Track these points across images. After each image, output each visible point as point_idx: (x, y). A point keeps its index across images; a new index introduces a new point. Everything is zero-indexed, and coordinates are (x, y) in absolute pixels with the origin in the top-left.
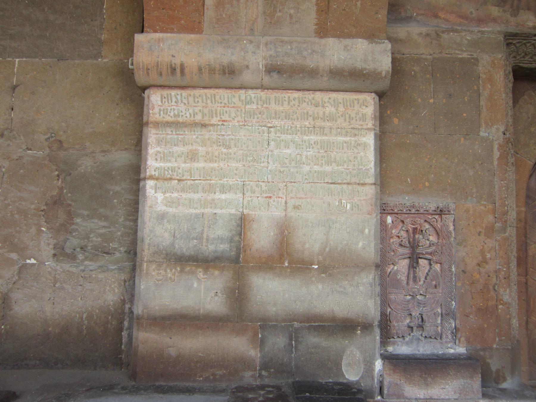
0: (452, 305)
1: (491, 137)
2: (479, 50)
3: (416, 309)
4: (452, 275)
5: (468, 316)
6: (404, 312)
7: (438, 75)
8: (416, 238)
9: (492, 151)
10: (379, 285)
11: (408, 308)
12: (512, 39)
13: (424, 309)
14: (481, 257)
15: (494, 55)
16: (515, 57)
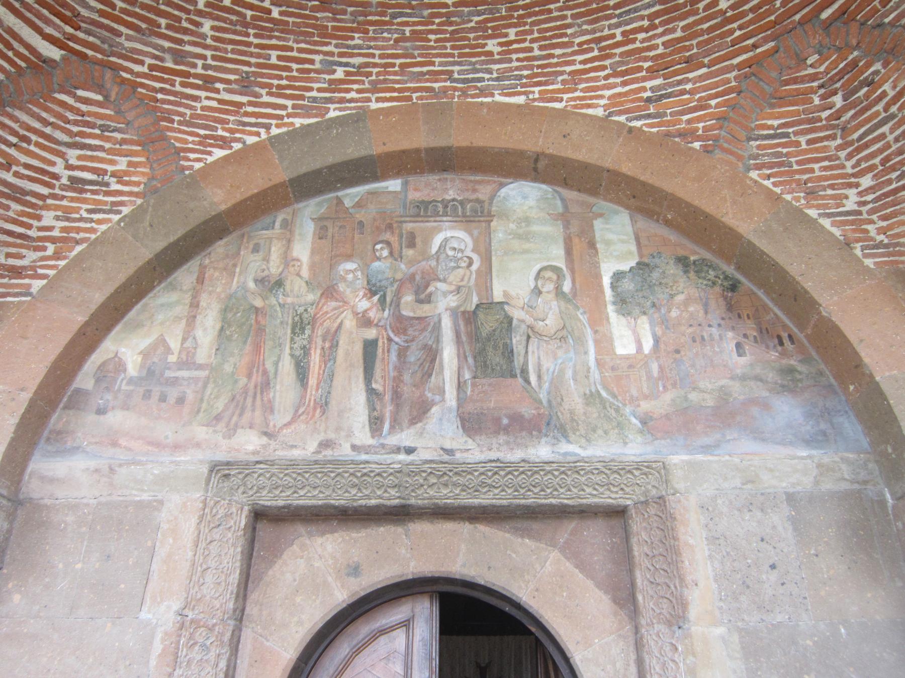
1: (155, 621)
2: (167, 489)
7: (98, 527)
9: (151, 643)
12: (229, 469)
15: (189, 495)
16: (244, 493)
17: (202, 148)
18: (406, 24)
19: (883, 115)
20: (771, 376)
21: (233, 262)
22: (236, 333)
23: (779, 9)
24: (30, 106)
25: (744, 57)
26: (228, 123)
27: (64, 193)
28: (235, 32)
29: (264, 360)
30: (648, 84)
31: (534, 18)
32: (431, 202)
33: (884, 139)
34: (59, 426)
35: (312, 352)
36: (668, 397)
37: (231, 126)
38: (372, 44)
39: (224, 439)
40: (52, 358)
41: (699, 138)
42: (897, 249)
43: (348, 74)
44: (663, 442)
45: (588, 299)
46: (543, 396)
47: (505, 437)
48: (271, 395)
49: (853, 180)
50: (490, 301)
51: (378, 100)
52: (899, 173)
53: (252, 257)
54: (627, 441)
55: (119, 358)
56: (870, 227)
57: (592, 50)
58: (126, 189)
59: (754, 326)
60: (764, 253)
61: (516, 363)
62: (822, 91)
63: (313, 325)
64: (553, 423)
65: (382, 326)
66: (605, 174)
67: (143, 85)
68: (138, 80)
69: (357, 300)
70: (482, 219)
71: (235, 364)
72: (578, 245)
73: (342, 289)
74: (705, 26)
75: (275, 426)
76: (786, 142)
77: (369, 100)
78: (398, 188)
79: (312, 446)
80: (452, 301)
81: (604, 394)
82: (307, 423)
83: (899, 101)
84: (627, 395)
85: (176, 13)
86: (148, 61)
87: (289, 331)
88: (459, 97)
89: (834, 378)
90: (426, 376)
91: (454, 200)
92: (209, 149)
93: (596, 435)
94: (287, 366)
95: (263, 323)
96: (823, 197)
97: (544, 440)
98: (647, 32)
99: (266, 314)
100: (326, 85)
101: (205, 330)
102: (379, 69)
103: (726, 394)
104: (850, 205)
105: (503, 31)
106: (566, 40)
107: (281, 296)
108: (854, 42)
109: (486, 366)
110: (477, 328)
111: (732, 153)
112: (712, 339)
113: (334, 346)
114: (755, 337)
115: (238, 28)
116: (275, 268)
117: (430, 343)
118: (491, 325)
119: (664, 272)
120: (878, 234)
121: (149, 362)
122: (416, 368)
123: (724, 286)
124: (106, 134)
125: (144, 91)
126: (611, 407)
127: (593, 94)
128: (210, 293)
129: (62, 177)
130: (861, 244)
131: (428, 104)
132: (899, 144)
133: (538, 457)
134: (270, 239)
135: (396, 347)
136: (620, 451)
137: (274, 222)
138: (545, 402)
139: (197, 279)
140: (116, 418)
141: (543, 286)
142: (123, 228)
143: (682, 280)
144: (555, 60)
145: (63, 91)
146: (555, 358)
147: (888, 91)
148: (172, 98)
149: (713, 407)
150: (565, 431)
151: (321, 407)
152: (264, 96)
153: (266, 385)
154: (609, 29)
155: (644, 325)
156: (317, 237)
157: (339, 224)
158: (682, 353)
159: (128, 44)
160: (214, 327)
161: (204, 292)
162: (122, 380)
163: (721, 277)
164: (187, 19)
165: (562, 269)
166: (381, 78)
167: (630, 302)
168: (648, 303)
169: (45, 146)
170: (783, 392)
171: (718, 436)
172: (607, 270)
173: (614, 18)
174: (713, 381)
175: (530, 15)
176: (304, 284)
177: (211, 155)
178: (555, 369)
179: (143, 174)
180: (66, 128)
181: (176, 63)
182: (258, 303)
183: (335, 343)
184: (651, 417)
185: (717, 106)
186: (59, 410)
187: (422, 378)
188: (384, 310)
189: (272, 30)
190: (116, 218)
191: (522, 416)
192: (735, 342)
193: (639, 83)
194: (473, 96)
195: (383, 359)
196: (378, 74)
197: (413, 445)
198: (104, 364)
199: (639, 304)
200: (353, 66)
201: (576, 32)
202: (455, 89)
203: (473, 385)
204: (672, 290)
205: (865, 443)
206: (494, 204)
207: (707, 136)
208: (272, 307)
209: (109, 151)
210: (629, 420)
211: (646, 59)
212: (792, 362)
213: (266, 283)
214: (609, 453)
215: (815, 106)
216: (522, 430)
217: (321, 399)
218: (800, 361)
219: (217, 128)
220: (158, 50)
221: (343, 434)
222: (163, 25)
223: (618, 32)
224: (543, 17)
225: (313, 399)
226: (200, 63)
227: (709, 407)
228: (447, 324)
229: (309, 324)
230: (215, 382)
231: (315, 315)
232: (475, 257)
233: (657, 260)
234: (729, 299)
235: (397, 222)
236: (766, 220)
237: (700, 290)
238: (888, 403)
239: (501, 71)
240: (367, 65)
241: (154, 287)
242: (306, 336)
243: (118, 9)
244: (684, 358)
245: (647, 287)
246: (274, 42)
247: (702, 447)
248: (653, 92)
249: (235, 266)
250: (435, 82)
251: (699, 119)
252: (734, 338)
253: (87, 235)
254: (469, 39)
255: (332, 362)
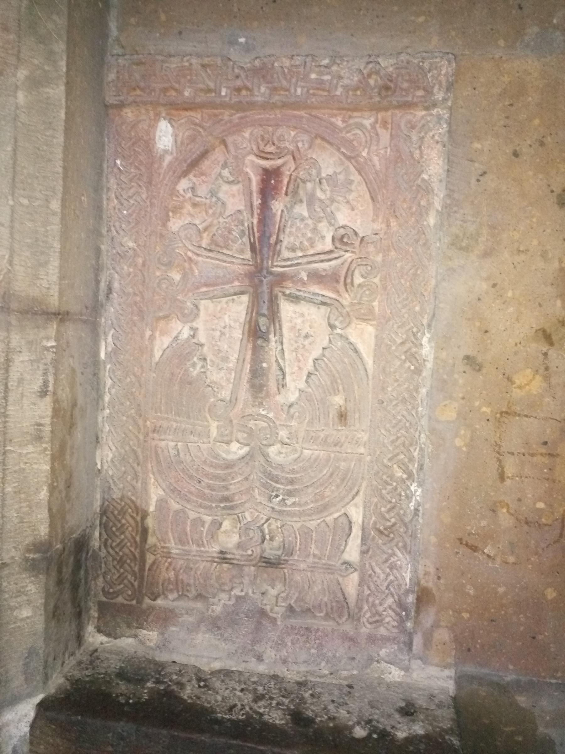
0: (409, 498)
3: (259, 498)
4: (418, 371)
5: (474, 549)
6: (211, 507)
8: (275, 215)
10: (43, 393)
11: (226, 493)
13: (289, 502)
14: (559, 303)
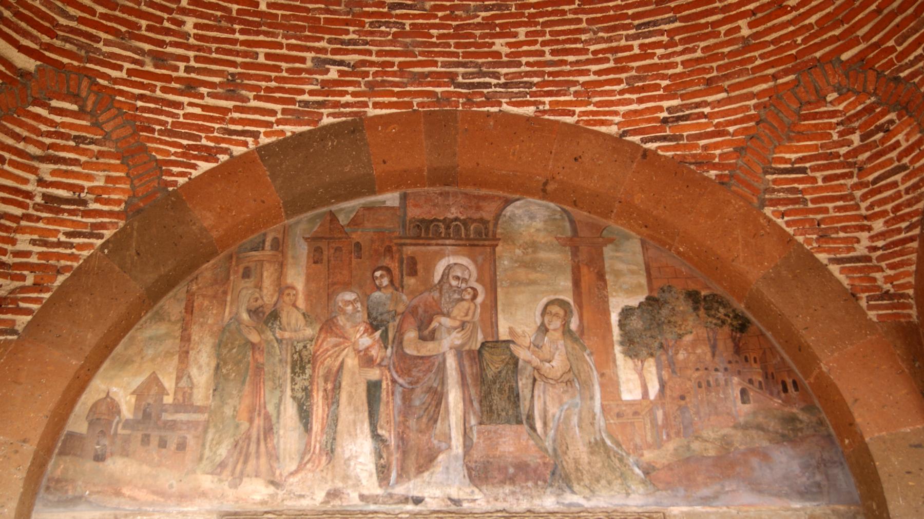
17: (185, 160)
18: (406, 16)
19: (896, 164)
20: (773, 425)
21: (222, 289)
22: (233, 372)
23: (799, 45)
24: (5, 123)
25: (764, 86)
26: (213, 132)
27: (39, 214)
28: (220, 29)
29: (265, 403)
30: (666, 104)
31: (546, 19)
32: (432, 221)
33: (895, 188)
34: (58, 473)
35: (315, 394)
36: (671, 446)
37: (216, 134)
38: (369, 38)
39: (230, 487)
40: (51, 406)
41: (715, 166)
42: (902, 301)
43: (342, 73)
44: (664, 493)
45: (595, 338)
46: (548, 444)
47: (512, 488)
48: (275, 441)
49: (865, 222)
50: (495, 340)
51: (376, 105)
52: (907, 224)
53: (244, 283)
54: (630, 492)
55: (112, 399)
56: (878, 275)
57: (607, 60)
58: (106, 208)
59: (760, 371)
60: (773, 304)
61: (522, 408)
62: (840, 128)
63: (313, 364)
64: (558, 472)
65: (385, 366)
66: (617, 204)
67: (121, 93)
68: (117, 87)
69: (358, 336)
70: (486, 243)
71: (235, 407)
72: (587, 276)
73: (341, 323)
74: (726, 50)
75: (281, 475)
76: (803, 177)
77: (365, 105)
78: (396, 203)
79: (320, 496)
80: (456, 338)
81: (609, 442)
82: (313, 471)
83: (910, 154)
84: (632, 443)
85: (159, 13)
86: (127, 65)
87: (289, 371)
88: (464, 104)
89: (833, 428)
90: (432, 422)
91: (456, 219)
92: (193, 161)
93: (600, 486)
94: (290, 410)
95: (261, 360)
96: (835, 240)
97: (549, 490)
98: (666, 48)
99: (263, 351)
100: (318, 87)
101: (200, 368)
102: (377, 69)
103: (727, 444)
104: (861, 250)
105: (513, 30)
106: (580, 46)
107: (277, 330)
108: (871, 88)
109: (491, 410)
110: (482, 369)
111: (749, 186)
112: (718, 385)
113: (337, 387)
114: (760, 383)
115: (224, 24)
116: (268, 297)
117: (435, 385)
118: (497, 366)
119: (673, 309)
120: (886, 283)
121: (144, 403)
122: (422, 412)
123: (733, 326)
124: (81, 146)
125: (123, 99)
126: (615, 456)
127: (607, 109)
128: (202, 325)
129: (35, 195)
130: (867, 294)
131: (431, 113)
132: (908, 197)
133: (543, 508)
134: (261, 262)
135: (400, 389)
136: (622, 502)
137: (264, 242)
138: (550, 450)
139: (186, 309)
140: (116, 465)
141: (550, 322)
142: (107, 255)
143: (691, 318)
144: (568, 68)
145: (37, 102)
146: (561, 403)
147: (902, 142)
148: (152, 105)
149: (713, 457)
150: (570, 481)
151: (327, 454)
152: (252, 101)
153: (269, 430)
154: (627, 40)
155: (651, 367)
156: (312, 261)
157: (333, 245)
158: (688, 399)
159: (106, 49)
160: (208, 365)
161: (194, 324)
162: (118, 423)
163: (731, 315)
164: (168, 20)
165: (569, 304)
166: (379, 79)
167: (638, 342)
168: (656, 344)
169: (18, 163)
170: (784, 441)
171: (717, 487)
172: (617, 304)
173: (632, 29)
174: (716, 429)
175: (542, 15)
176: (301, 317)
177: (196, 169)
178: (560, 416)
179: (123, 191)
180: (38, 141)
181: (156, 66)
182: (254, 338)
183: (337, 384)
184: (654, 467)
185: (736, 133)
186: (54, 456)
187: (427, 424)
188: (386, 348)
189: (259, 24)
190: (99, 242)
191: (528, 465)
192: (740, 388)
193: (655, 102)
194: (479, 105)
195: (388, 402)
196: (376, 74)
197: (420, 495)
198: (95, 405)
199: (647, 346)
200: (348, 65)
201: (591, 40)
202: (460, 95)
203: (479, 432)
204: (681, 329)
205: (856, 494)
206: (499, 226)
207: (723, 165)
208: (268, 342)
209: (85, 165)
210: (632, 470)
211: (664, 77)
212: (795, 410)
213: (261, 315)
214: (611, 504)
215: (834, 141)
216: (527, 480)
217: (326, 445)
218: (802, 409)
219: (200, 137)
220: (138, 54)
221: (350, 483)
222: (144, 28)
223: (636, 43)
224: (556, 18)
225: (318, 446)
226: (182, 65)
227: (709, 457)
228: (451, 363)
229: (309, 362)
230: (215, 426)
231: (315, 353)
232: (480, 288)
233: (667, 295)
234: (737, 339)
235: (396, 244)
236: (777, 266)
237: (708, 329)
238: (874, 465)
239: (510, 76)
240: (363, 63)
241: (141, 318)
242: (307, 375)
243: (98, 15)
244: (689, 405)
245: (656, 325)
246: (261, 38)
247: (701, 498)
248: (670, 113)
249: (225, 293)
250: (438, 86)
251: (716, 146)
252: (739, 384)
253: (69, 263)
254: (474, 36)
255: (335, 405)
